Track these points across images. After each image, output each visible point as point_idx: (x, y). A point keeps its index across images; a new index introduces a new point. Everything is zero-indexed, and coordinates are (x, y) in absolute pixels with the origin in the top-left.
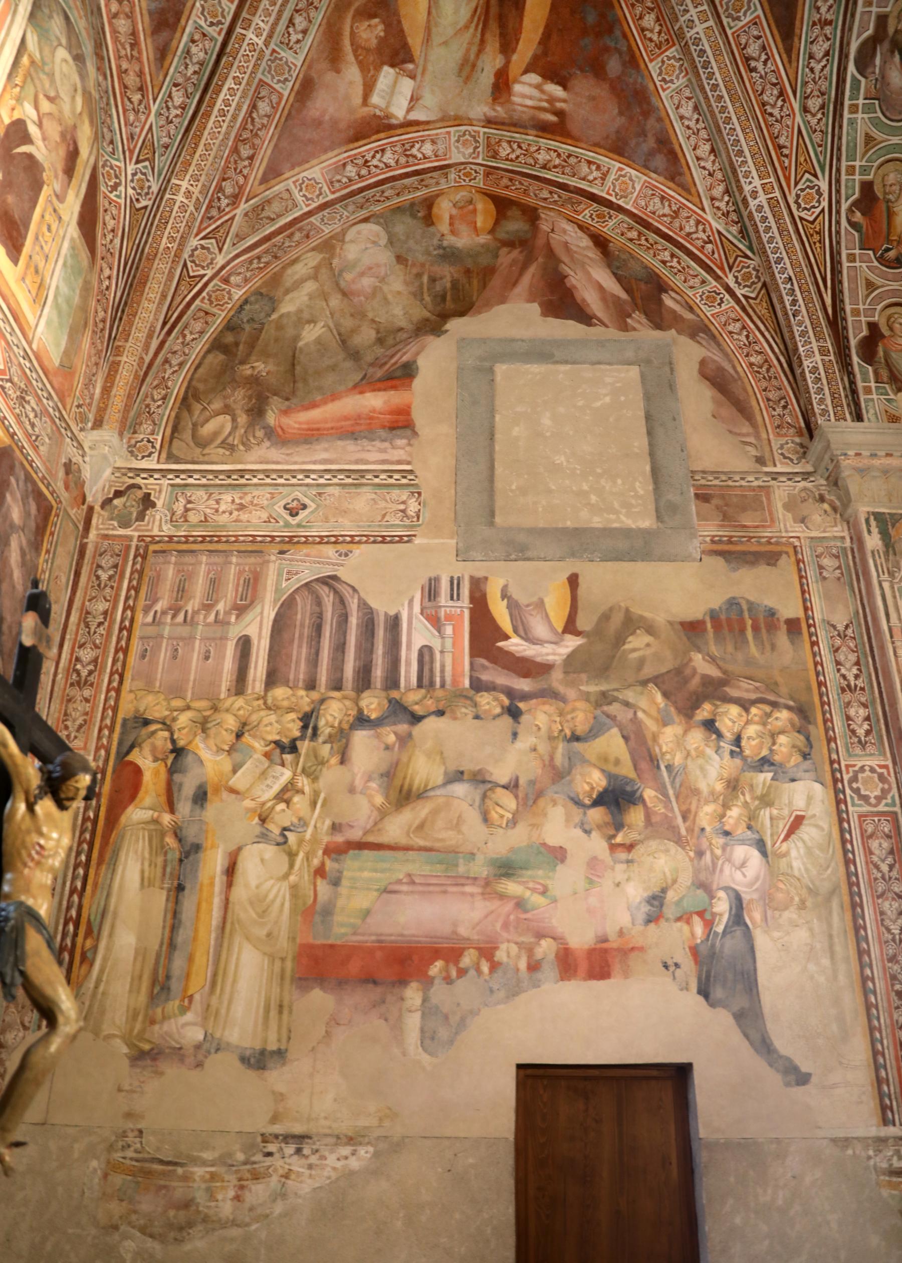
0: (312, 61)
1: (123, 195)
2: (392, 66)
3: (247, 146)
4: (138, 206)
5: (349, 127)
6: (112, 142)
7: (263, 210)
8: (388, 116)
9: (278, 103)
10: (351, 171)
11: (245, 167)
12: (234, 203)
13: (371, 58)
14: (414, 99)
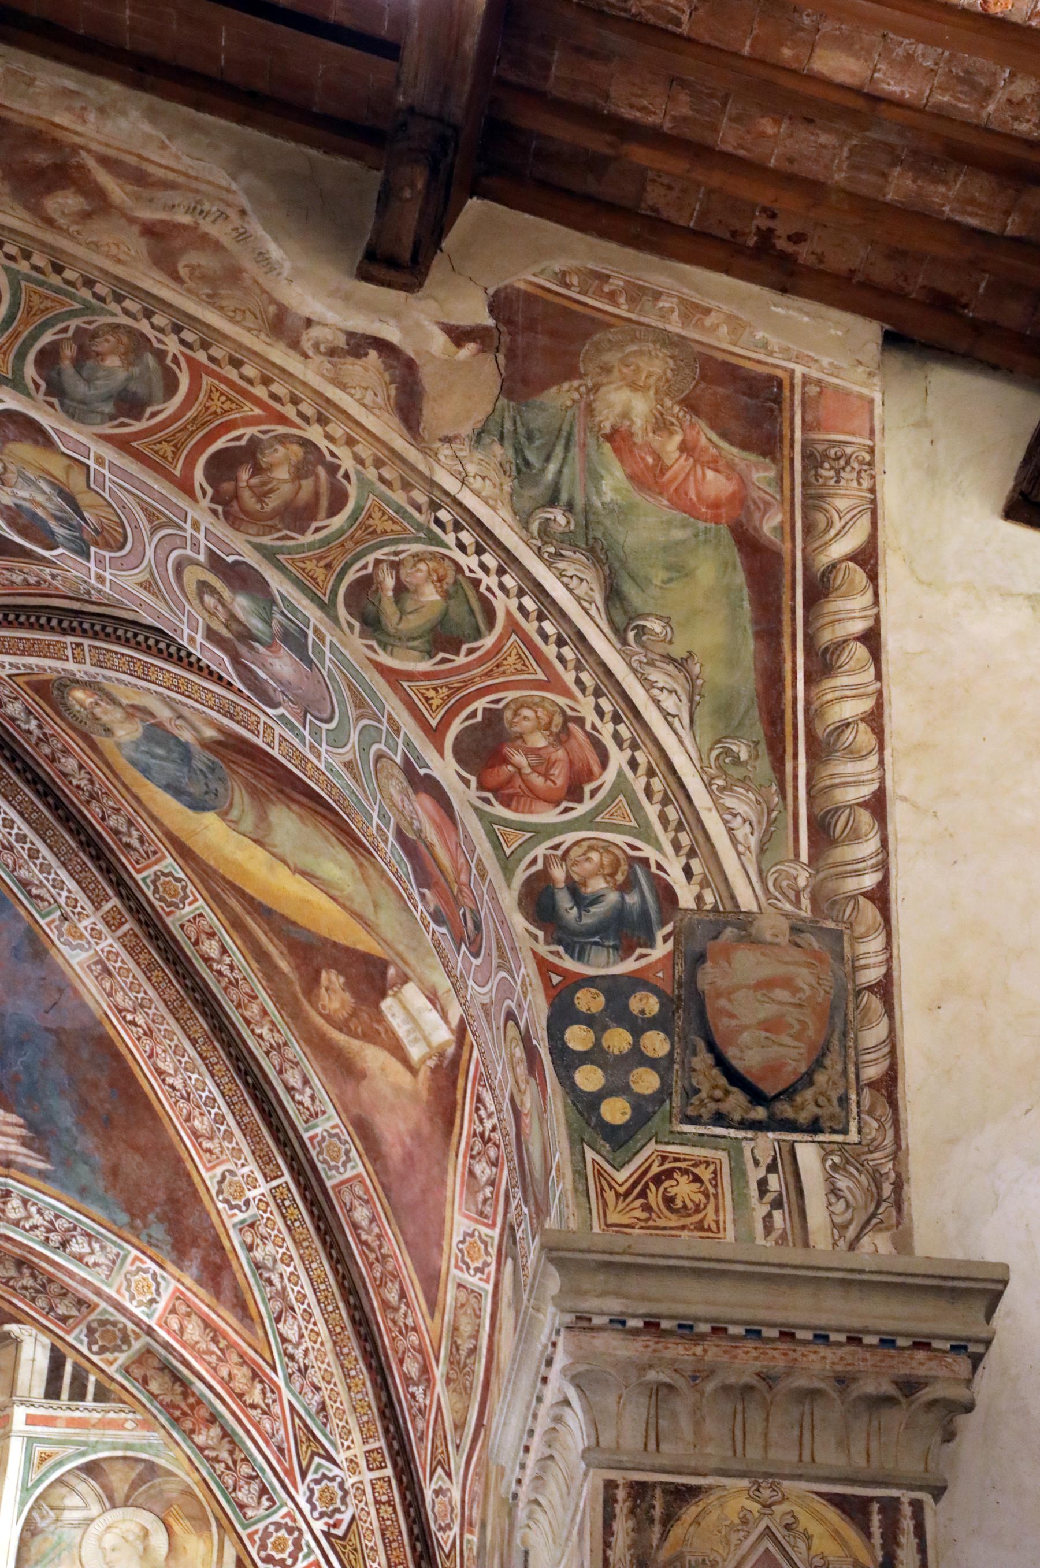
0: (339, 1098)
1: (313, 1544)
2: (383, 995)
3: (390, 1284)
4: (340, 1532)
5: (431, 1119)
6: (264, 1491)
7: (458, 1349)
8: (441, 1055)
9: (366, 1191)
10: (483, 1170)
11: (406, 1315)
12: (428, 1380)
13: (365, 1016)
14: (433, 998)
